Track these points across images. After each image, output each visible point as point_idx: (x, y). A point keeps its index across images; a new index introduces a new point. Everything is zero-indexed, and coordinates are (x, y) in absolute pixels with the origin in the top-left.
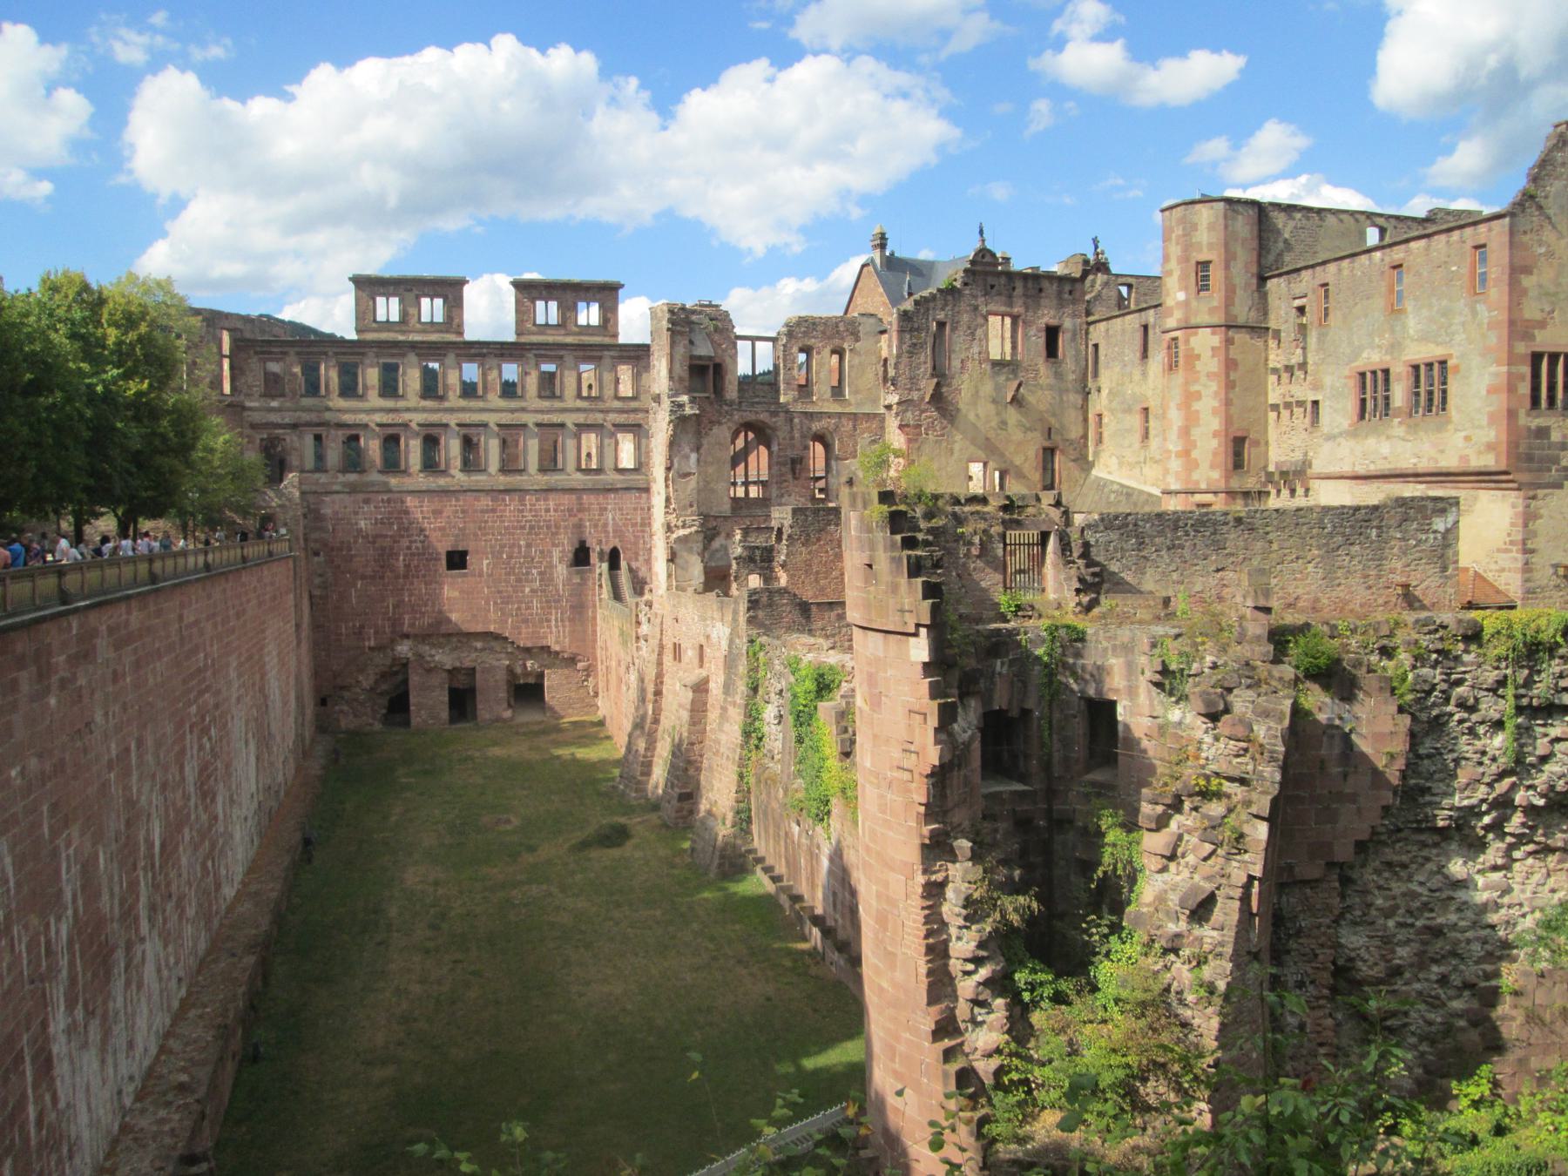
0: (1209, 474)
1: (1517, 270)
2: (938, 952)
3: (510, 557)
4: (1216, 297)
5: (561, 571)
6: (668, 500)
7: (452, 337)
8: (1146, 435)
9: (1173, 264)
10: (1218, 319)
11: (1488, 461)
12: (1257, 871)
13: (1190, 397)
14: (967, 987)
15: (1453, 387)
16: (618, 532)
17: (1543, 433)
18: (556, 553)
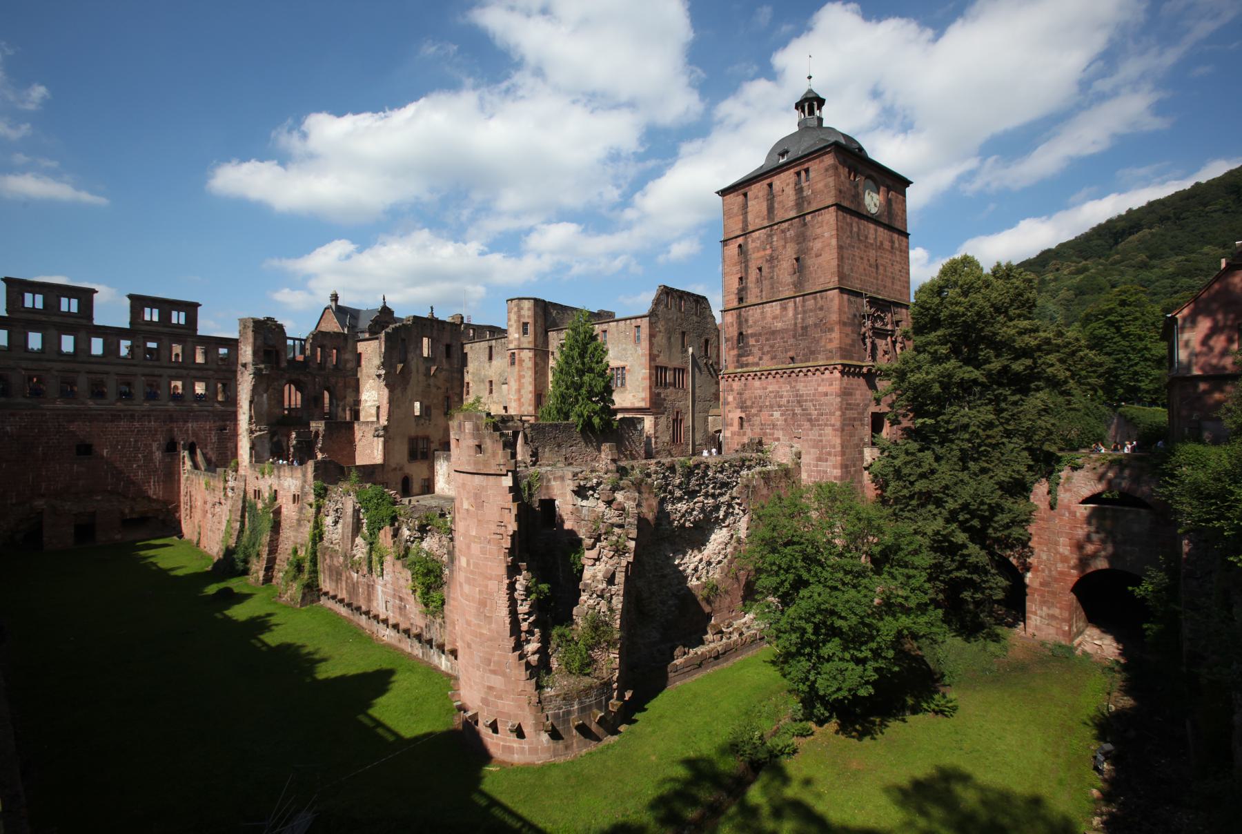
0: (528, 408)
1: (652, 336)
2: (513, 613)
3: (123, 447)
4: (530, 337)
5: (158, 455)
6: (251, 418)
7: (84, 322)
8: (491, 392)
9: (512, 322)
10: (531, 346)
11: (642, 405)
12: (631, 559)
13: (521, 377)
14: (524, 626)
15: (628, 377)
16: (195, 434)
17: (659, 394)
18: (155, 446)
